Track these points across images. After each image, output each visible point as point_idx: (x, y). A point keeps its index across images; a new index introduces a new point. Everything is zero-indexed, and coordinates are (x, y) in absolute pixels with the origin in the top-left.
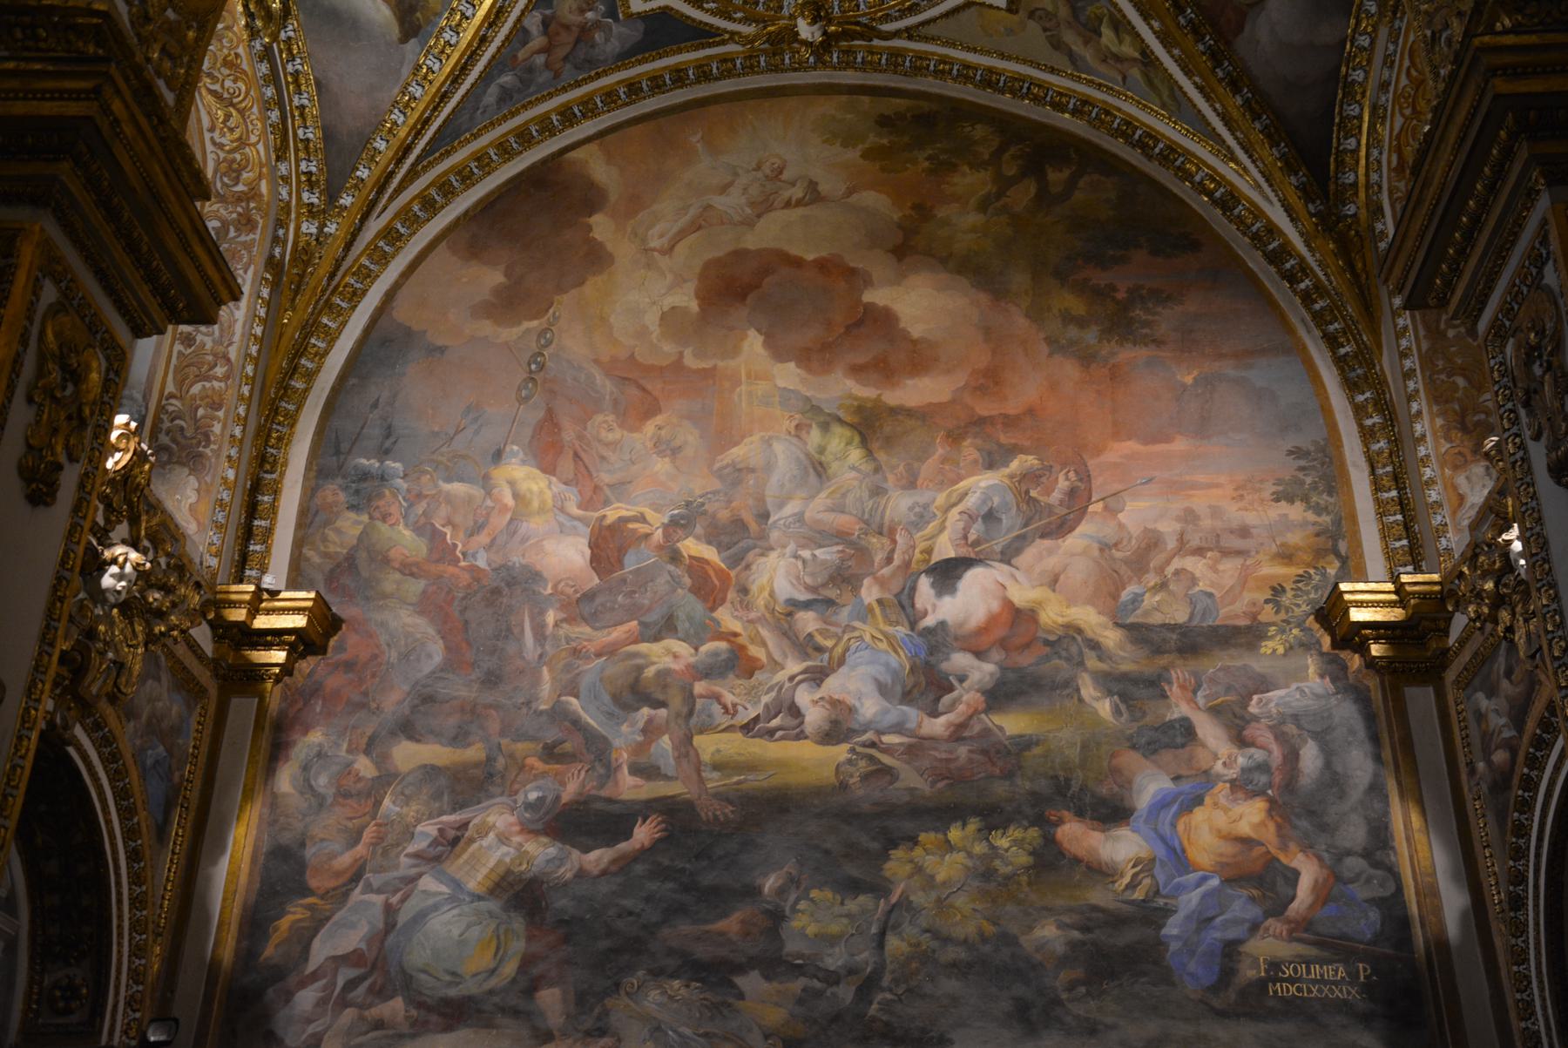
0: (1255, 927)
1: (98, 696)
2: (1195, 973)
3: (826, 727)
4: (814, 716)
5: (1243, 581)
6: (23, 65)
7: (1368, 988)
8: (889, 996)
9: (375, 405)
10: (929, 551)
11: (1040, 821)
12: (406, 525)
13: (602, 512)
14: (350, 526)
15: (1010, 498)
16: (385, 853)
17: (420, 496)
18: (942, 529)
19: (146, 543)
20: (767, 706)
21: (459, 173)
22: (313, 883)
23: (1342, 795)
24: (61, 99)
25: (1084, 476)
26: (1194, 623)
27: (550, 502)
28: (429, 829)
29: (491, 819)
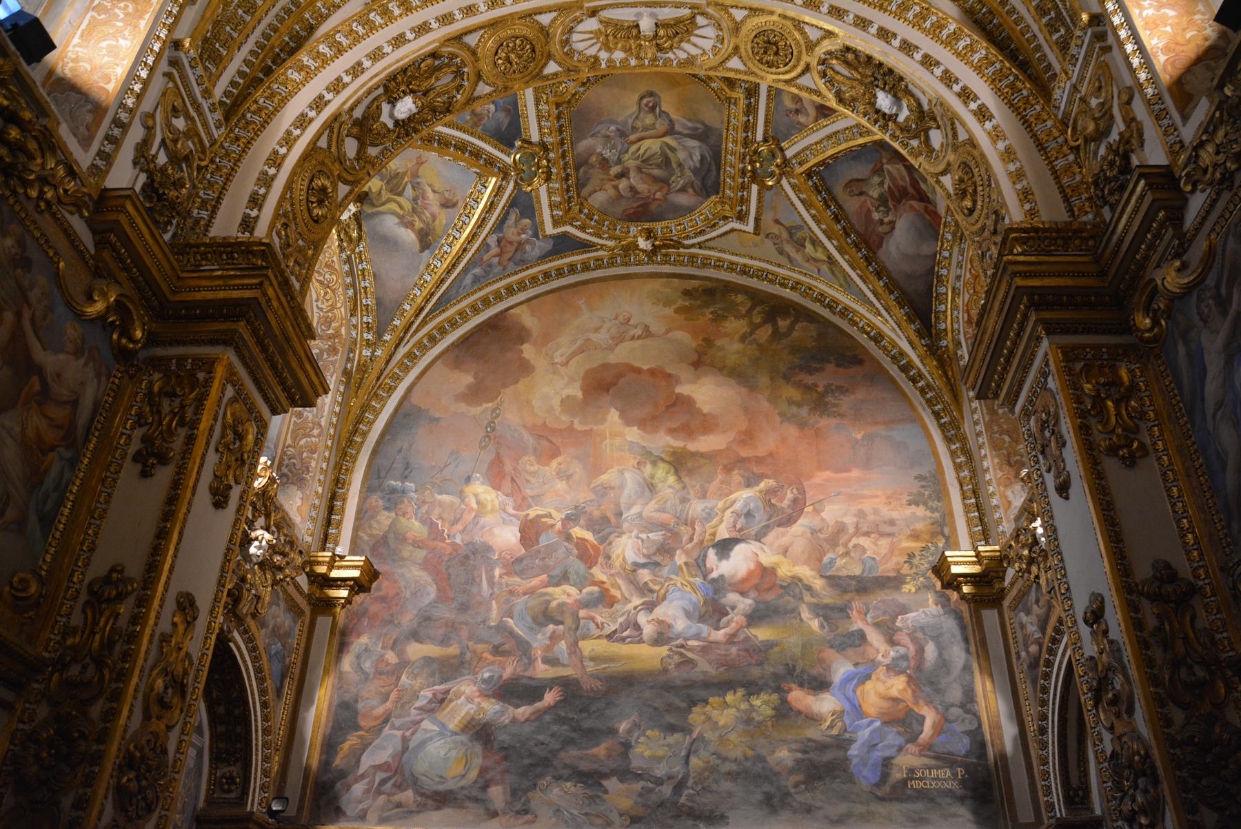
0: (900, 749)
1: (246, 614)
2: (867, 776)
3: (655, 636)
4: (648, 630)
6: (225, 273)
7: (963, 782)
8: (692, 792)
9: (400, 451)
10: (714, 534)
11: (778, 690)
12: (416, 519)
13: (527, 512)
14: (385, 519)
15: (760, 503)
16: (402, 706)
17: (424, 502)
18: (721, 521)
19: (273, 528)
20: (621, 624)
21: (449, 322)
22: (362, 723)
23: (948, 673)
24: (243, 289)
25: (802, 492)
26: (865, 575)
27: (497, 507)
28: (427, 694)
29: (462, 688)
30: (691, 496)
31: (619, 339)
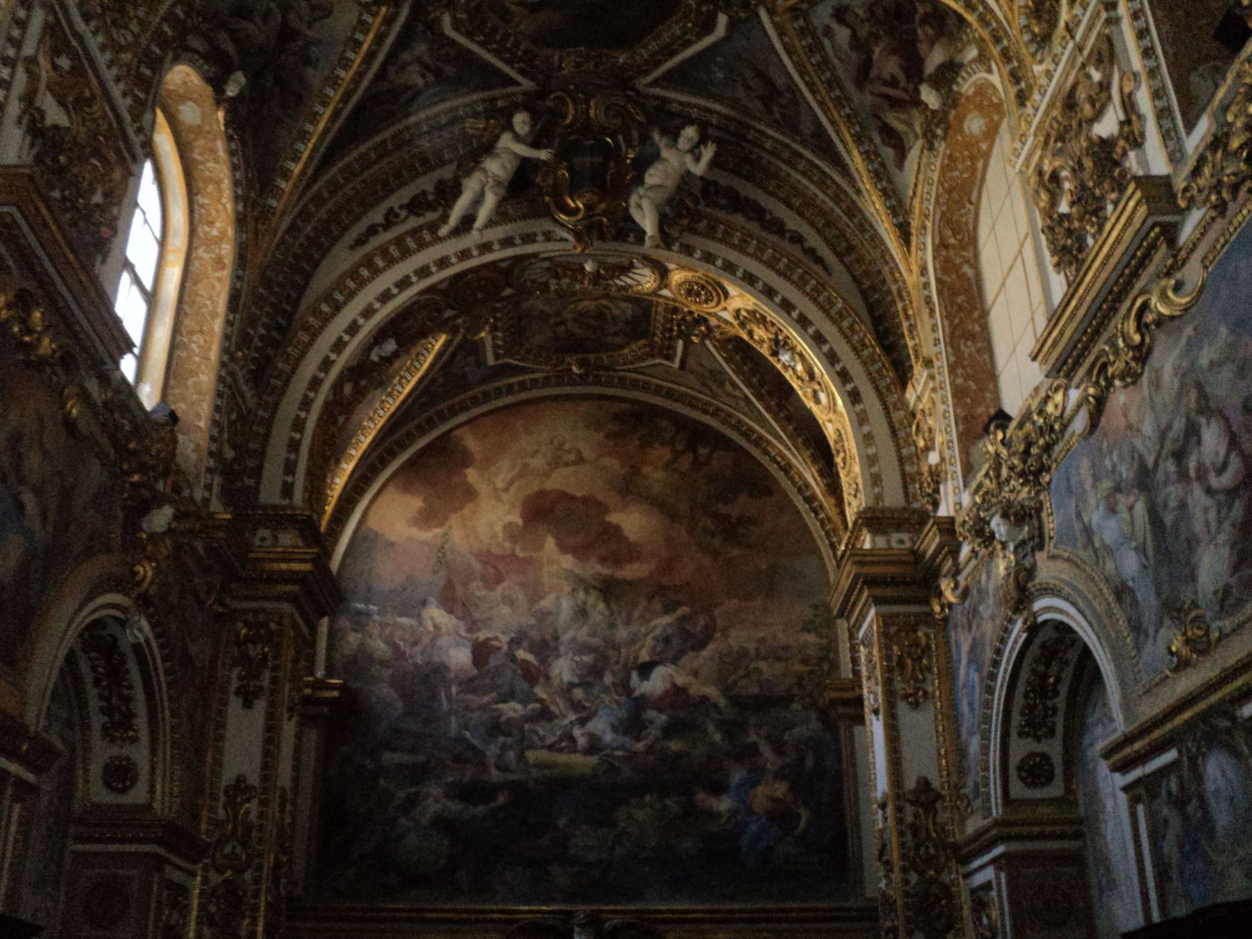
4: (582, 741)
10: (636, 658)
18: (643, 646)
25: (714, 620)
28: (401, 795)
30: (618, 621)
31: (555, 464)
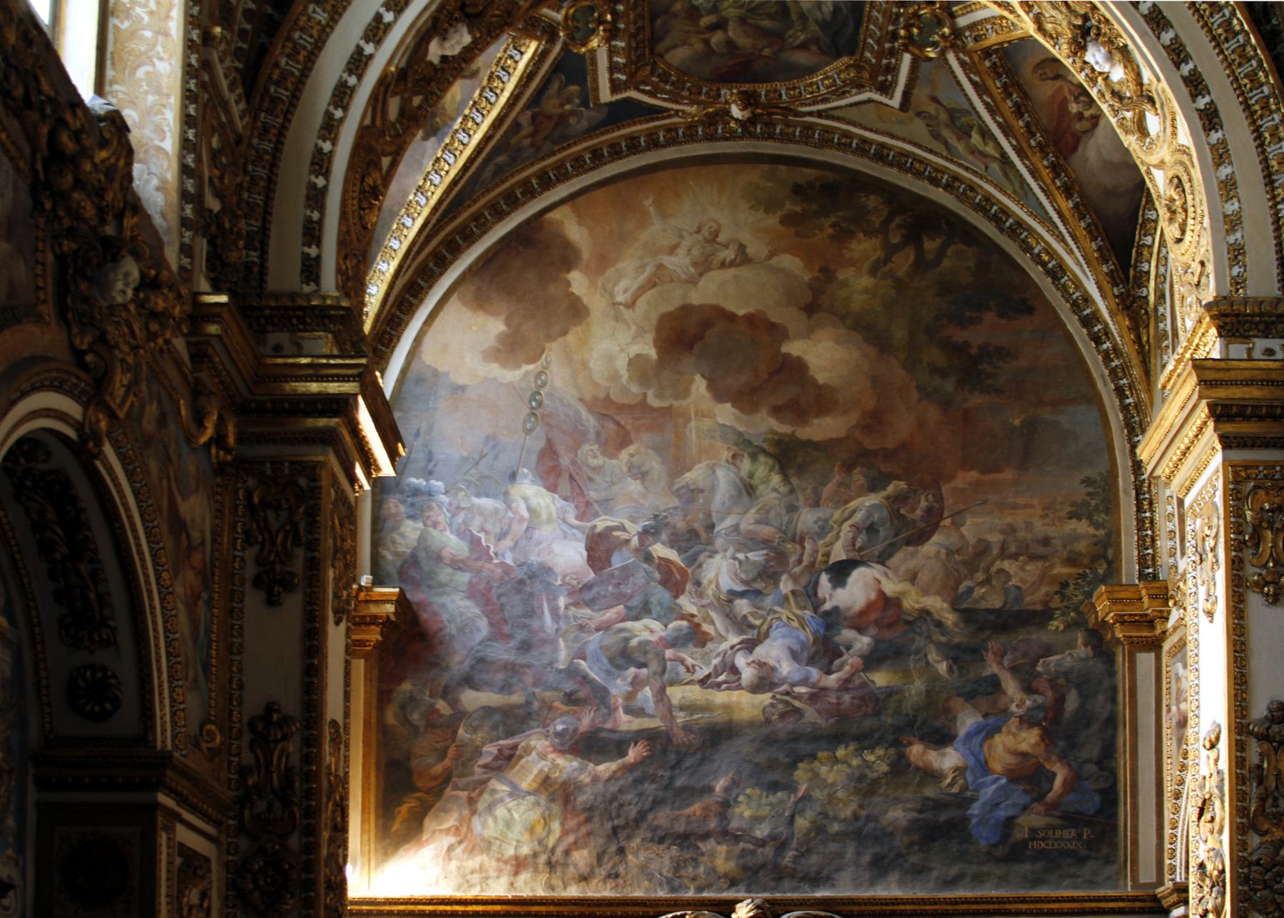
4: (748, 674)
5: (1042, 577)
10: (827, 555)
18: (837, 537)
25: (940, 499)
31: (704, 266)
